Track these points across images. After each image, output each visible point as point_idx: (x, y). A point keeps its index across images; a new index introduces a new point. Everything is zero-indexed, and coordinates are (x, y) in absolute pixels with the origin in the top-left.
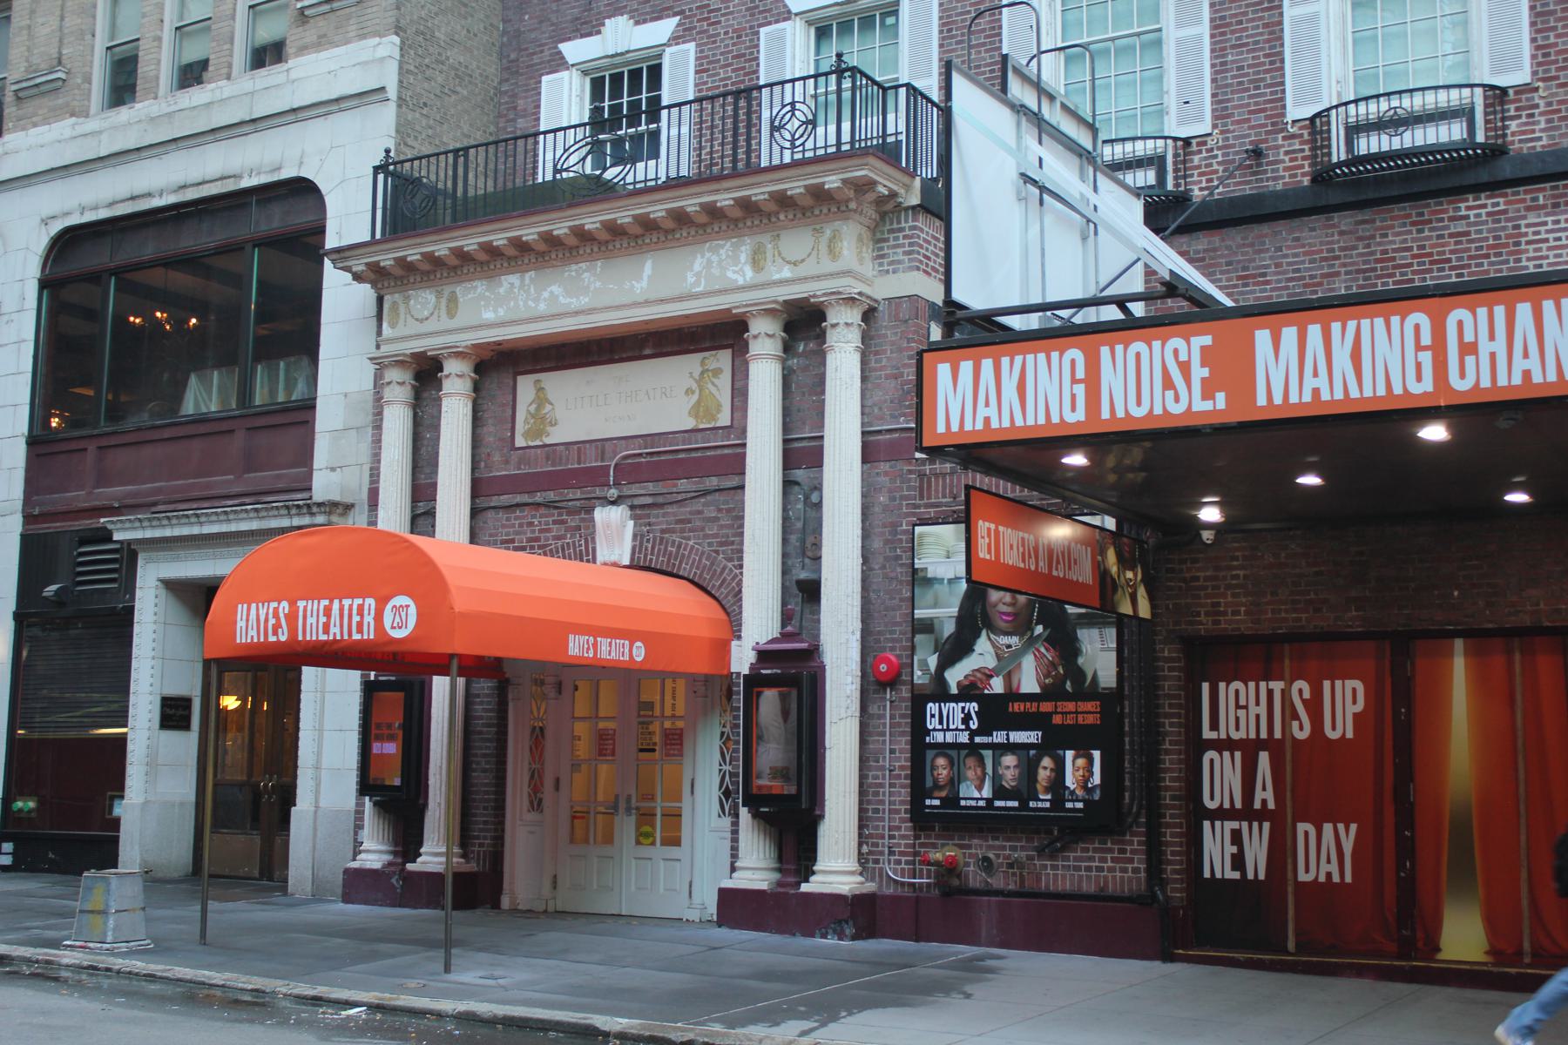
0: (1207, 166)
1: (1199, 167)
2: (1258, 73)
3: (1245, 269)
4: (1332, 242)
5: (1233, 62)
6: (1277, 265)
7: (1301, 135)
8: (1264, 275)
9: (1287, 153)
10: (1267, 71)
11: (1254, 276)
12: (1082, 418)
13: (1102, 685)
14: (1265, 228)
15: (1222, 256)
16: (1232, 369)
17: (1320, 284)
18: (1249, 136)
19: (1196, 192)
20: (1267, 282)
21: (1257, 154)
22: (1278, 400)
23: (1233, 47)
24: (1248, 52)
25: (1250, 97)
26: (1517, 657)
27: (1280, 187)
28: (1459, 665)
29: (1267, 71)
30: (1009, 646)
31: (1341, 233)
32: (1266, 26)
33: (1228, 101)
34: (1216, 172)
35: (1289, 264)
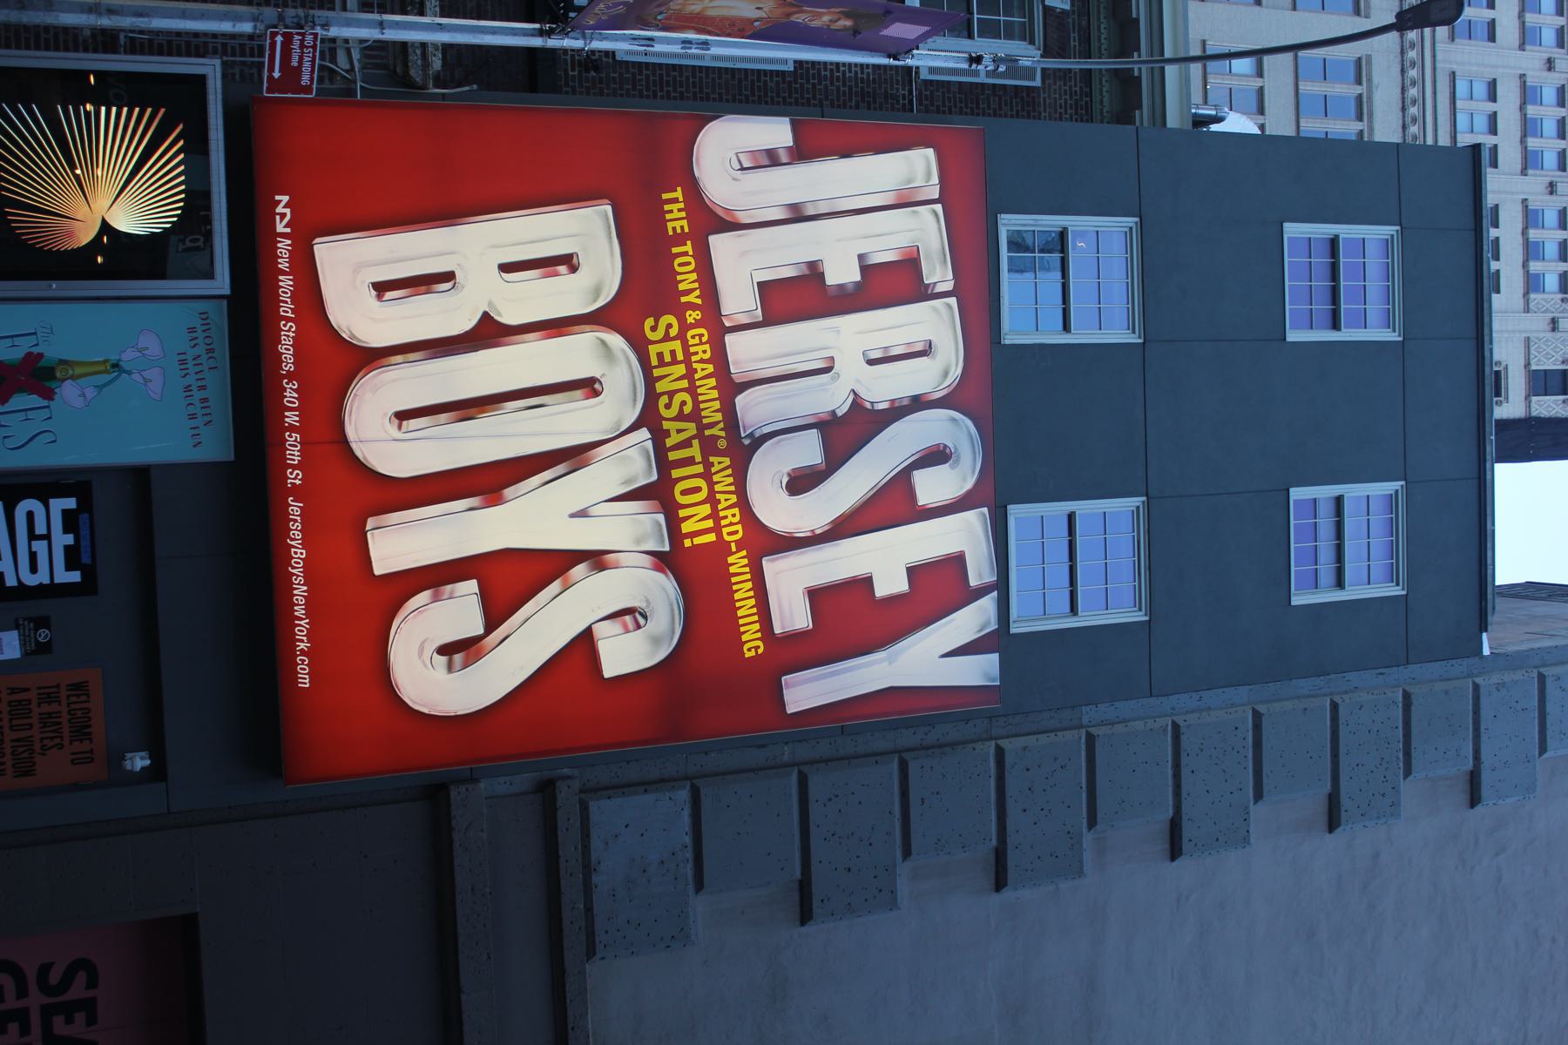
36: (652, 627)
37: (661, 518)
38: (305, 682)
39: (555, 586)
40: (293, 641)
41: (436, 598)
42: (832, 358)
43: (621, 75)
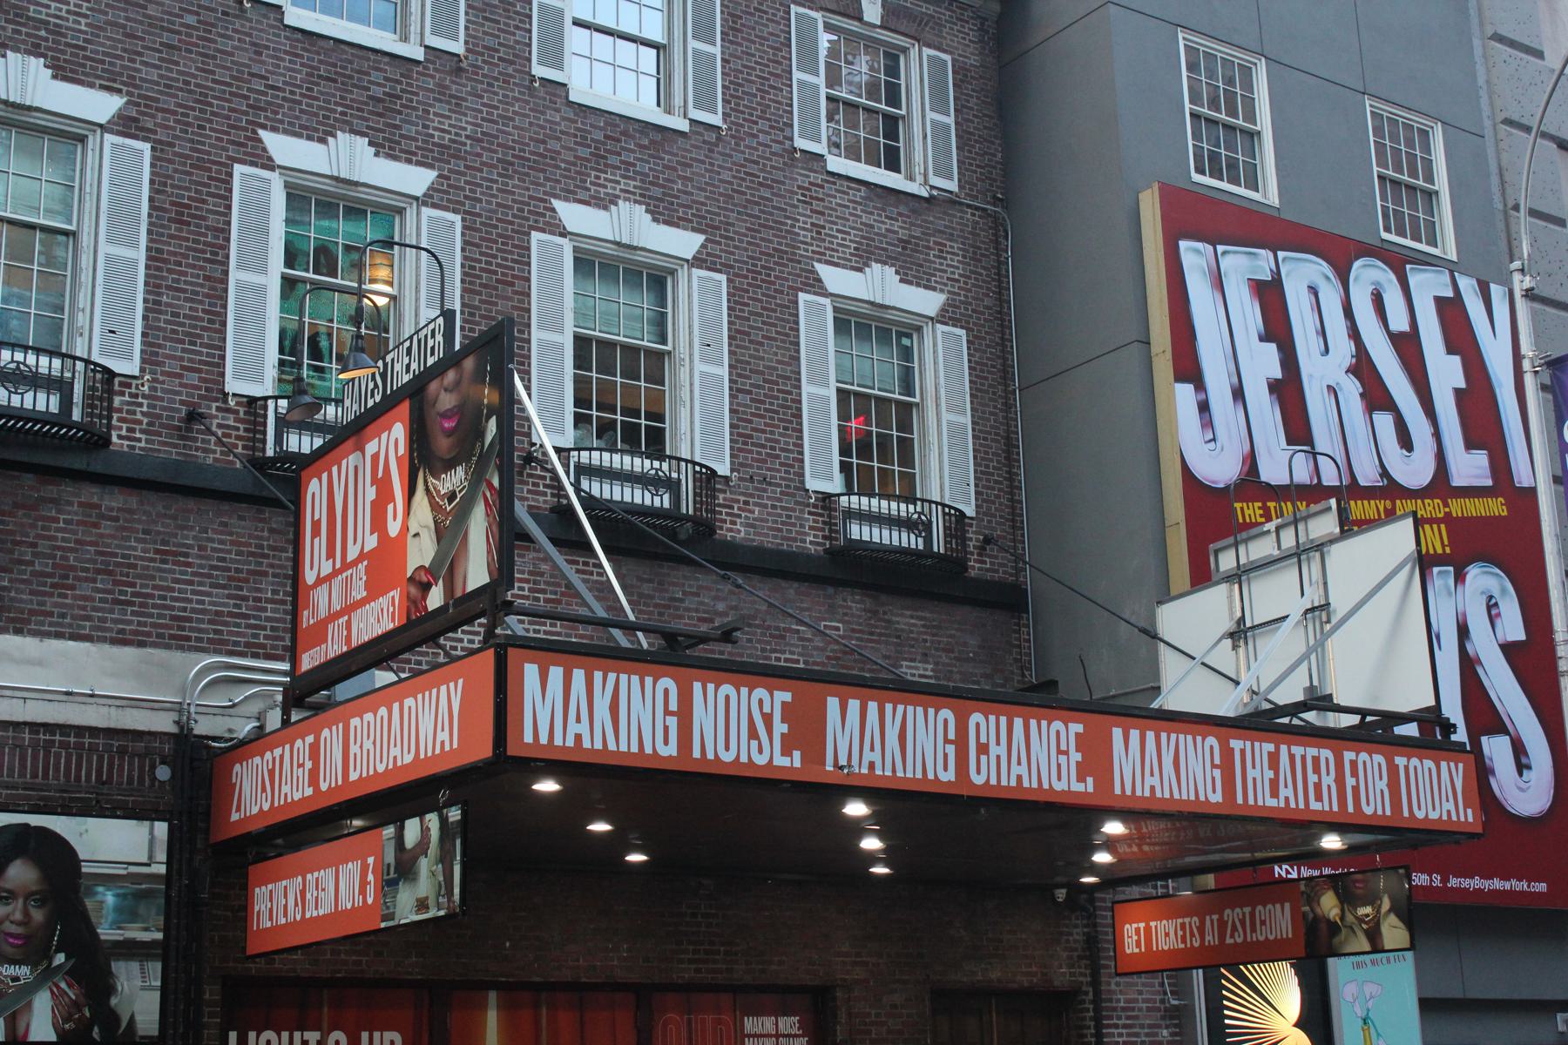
0: (128, 412)
1: (120, 410)
2: (195, 327)
3: (164, 543)
4: (261, 538)
5: (168, 305)
6: (201, 548)
7: (237, 412)
8: (186, 555)
9: (220, 426)
10: (203, 329)
11: (175, 554)
12: (675, 754)
13: (141, 1033)
14: (191, 503)
15: (140, 521)
16: (806, 731)
17: (247, 581)
18: (178, 393)
19: (115, 439)
20: (189, 565)
21: (193, 417)
22: (544, 740)
23: (169, 288)
24: (186, 300)
25: (184, 350)
26: (544, 1011)
27: (210, 461)
28: (492, 1017)
29: (203, 329)
30: (15, 979)
31: (272, 531)
32: (207, 278)
33: (160, 346)
34: (140, 422)
35: (214, 550)
36: (1496, 593)
37: (1436, 570)
38: (1542, 887)
39: (1480, 671)
40: (1522, 892)
41: (1493, 772)
42: (1329, 387)
43: (985, 514)
